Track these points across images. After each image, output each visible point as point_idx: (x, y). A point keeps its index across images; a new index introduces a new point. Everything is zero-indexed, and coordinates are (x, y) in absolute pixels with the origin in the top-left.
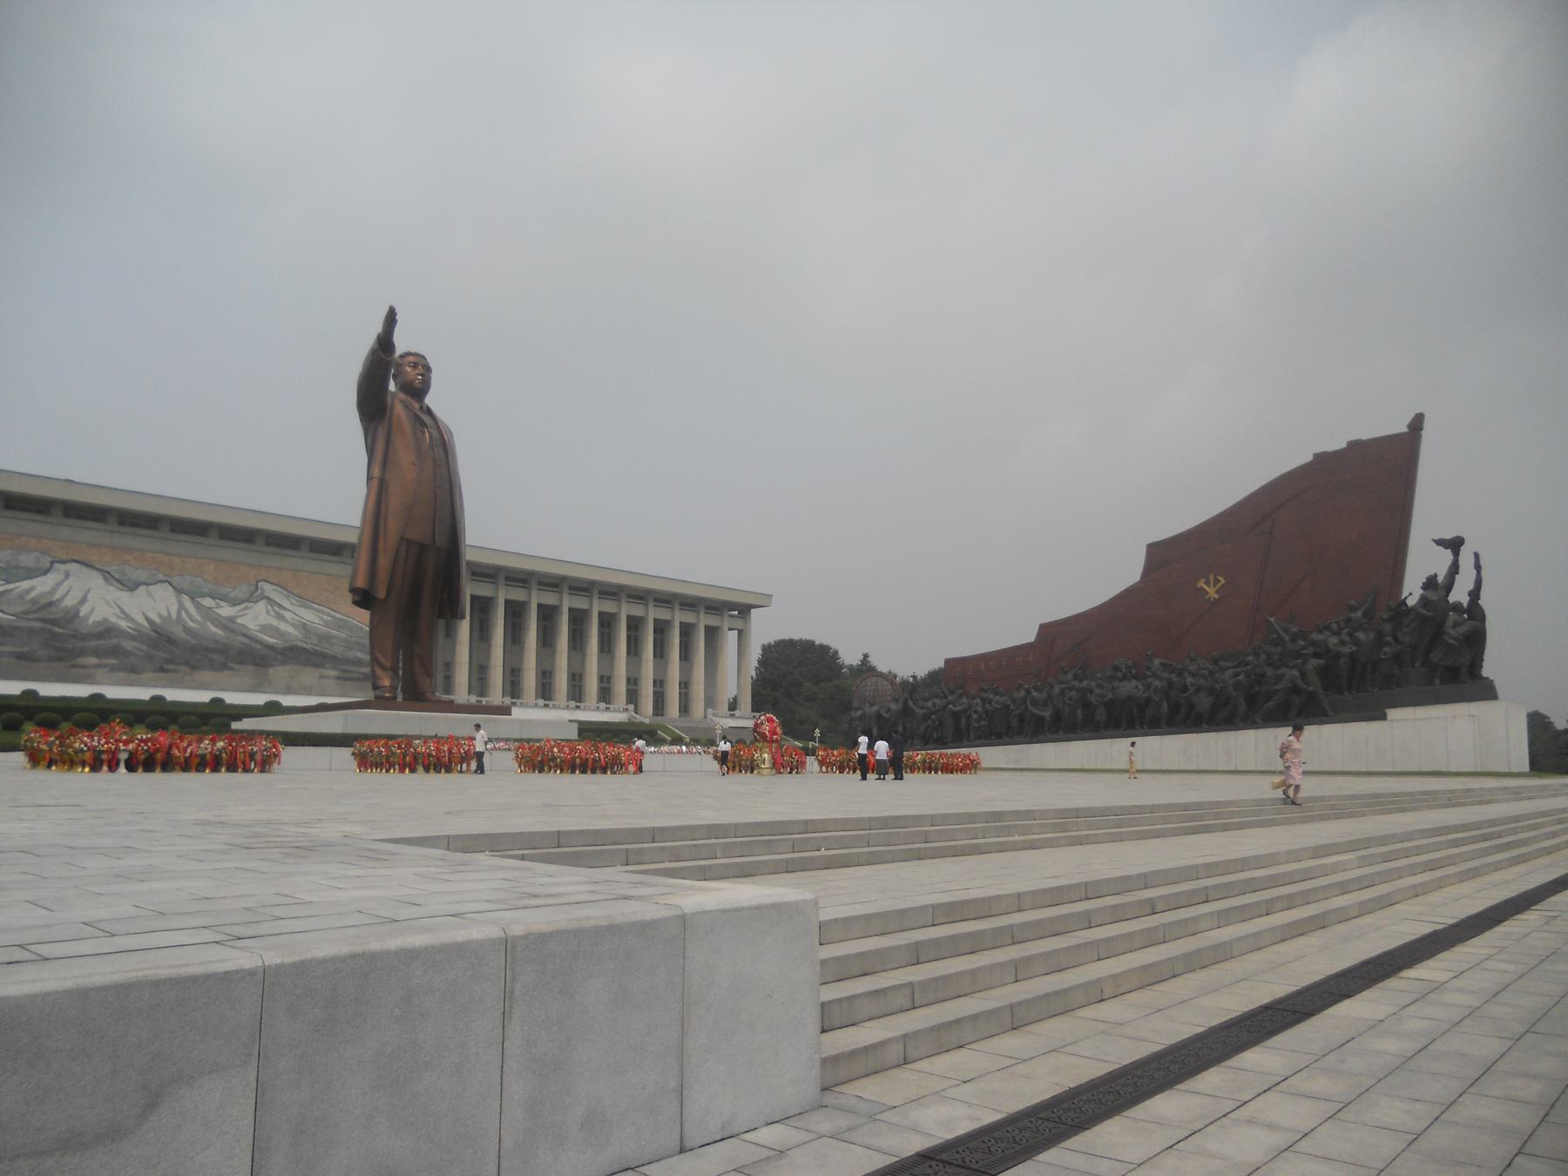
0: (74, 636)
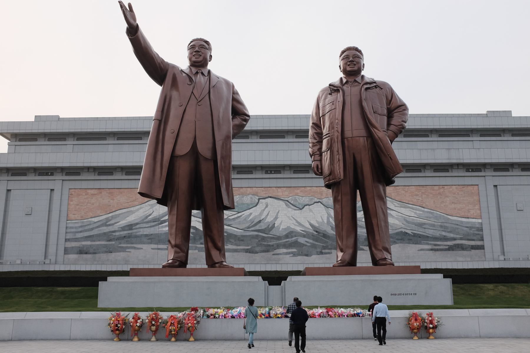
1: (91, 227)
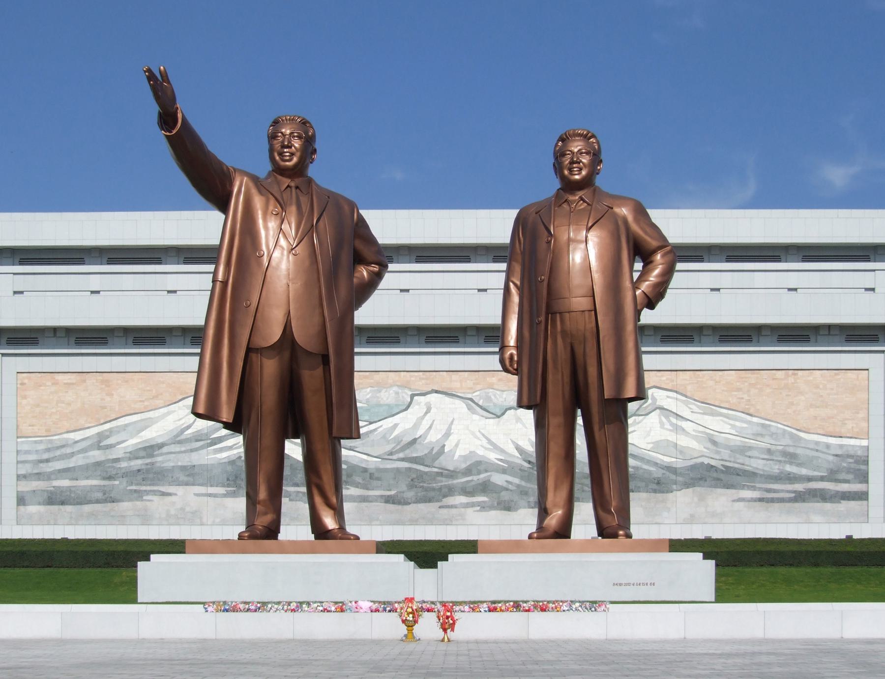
0: (441, 474)
1: (68, 450)
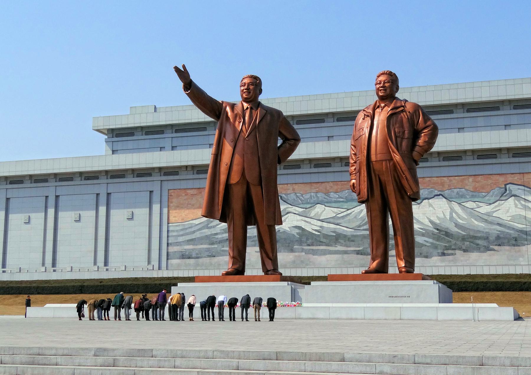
1: (193, 229)
